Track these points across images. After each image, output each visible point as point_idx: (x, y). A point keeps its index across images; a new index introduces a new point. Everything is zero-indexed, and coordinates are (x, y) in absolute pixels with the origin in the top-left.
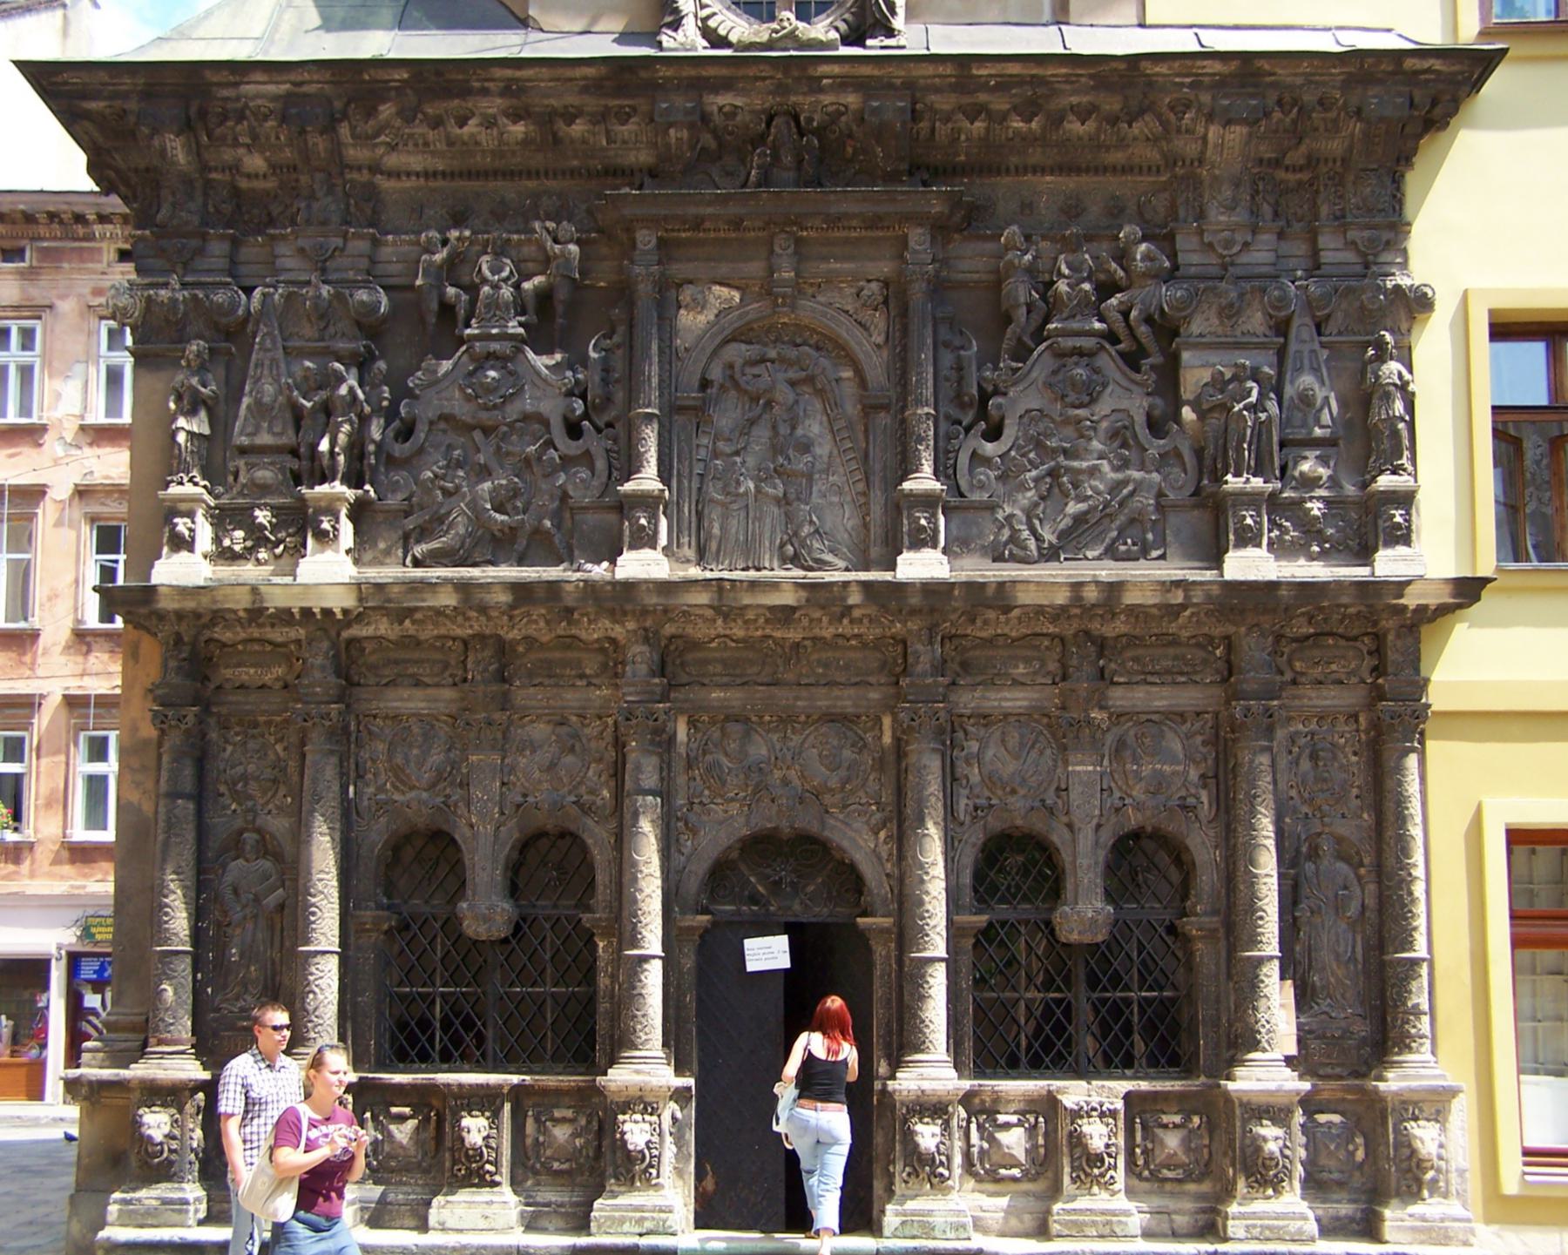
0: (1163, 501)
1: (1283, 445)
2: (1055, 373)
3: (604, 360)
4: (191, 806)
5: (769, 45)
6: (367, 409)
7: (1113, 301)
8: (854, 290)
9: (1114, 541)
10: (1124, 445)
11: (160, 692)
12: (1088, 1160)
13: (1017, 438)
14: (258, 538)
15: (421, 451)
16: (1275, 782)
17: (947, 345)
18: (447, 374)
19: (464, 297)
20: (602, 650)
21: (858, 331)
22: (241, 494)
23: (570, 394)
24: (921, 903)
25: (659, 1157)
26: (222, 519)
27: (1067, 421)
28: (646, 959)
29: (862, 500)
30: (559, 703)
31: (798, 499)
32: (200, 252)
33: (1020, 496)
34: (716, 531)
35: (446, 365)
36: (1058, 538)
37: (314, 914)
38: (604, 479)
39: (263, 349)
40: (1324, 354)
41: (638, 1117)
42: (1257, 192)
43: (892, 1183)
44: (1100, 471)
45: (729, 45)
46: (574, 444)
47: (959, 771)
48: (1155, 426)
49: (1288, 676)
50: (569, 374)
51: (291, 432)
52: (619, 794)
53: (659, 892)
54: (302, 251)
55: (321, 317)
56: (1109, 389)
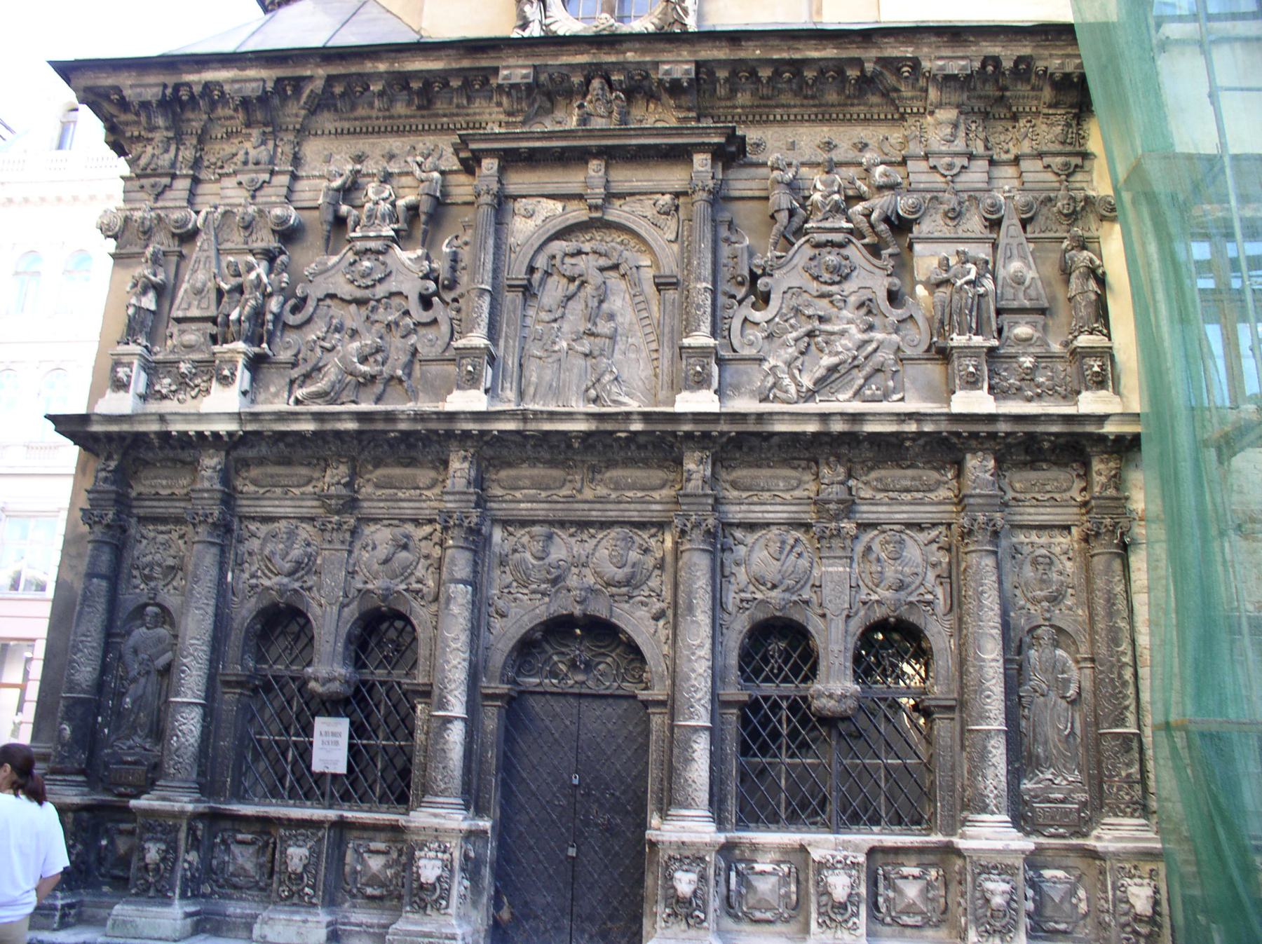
0: (901, 355)
1: (999, 312)
2: (811, 259)
3: (455, 254)
4: (104, 584)
6: (269, 289)
7: (859, 207)
9: (861, 387)
10: (869, 312)
11: (91, 496)
12: (833, 907)
13: (781, 308)
14: (183, 383)
15: (309, 321)
16: (1000, 582)
17: (727, 240)
18: (334, 266)
19: (355, 212)
20: (435, 468)
21: (652, 230)
22: (172, 352)
23: (426, 277)
24: (689, 679)
25: (449, 890)
26: (152, 369)
27: (822, 296)
28: (449, 720)
29: (655, 355)
30: (397, 511)
31: (601, 355)
32: (168, 187)
33: (782, 352)
34: (534, 379)
35: (335, 259)
36: (815, 384)
37: (183, 672)
38: (447, 340)
39: (201, 249)
40: (1032, 246)
41: (432, 854)
43: (655, 922)
44: (848, 331)
46: (425, 314)
47: (727, 573)
48: (894, 297)
49: (1010, 494)
50: (426, 263)
51: (213, 307)
52: (439, 584)
53: (466, 664)
54: (240, 183)
55: (246, 228)
56: (855, 274)
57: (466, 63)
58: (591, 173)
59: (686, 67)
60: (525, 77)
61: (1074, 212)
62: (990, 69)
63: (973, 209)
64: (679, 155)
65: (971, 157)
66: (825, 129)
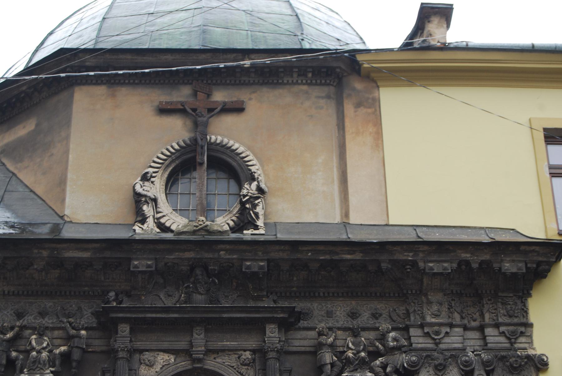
5: (194, 232)
8: (237, 356)
19: (21, 357)
42: (451, 306)
45: (172, 231)
57: (108, 254)
58: (195, 335)
59: (262, 264)
60: (149, 266)
61: (520, 365)
62: (463, 267)
63: (454, 364)
64: (256, 326)
65: (451, 326)
66: (353, 303)
